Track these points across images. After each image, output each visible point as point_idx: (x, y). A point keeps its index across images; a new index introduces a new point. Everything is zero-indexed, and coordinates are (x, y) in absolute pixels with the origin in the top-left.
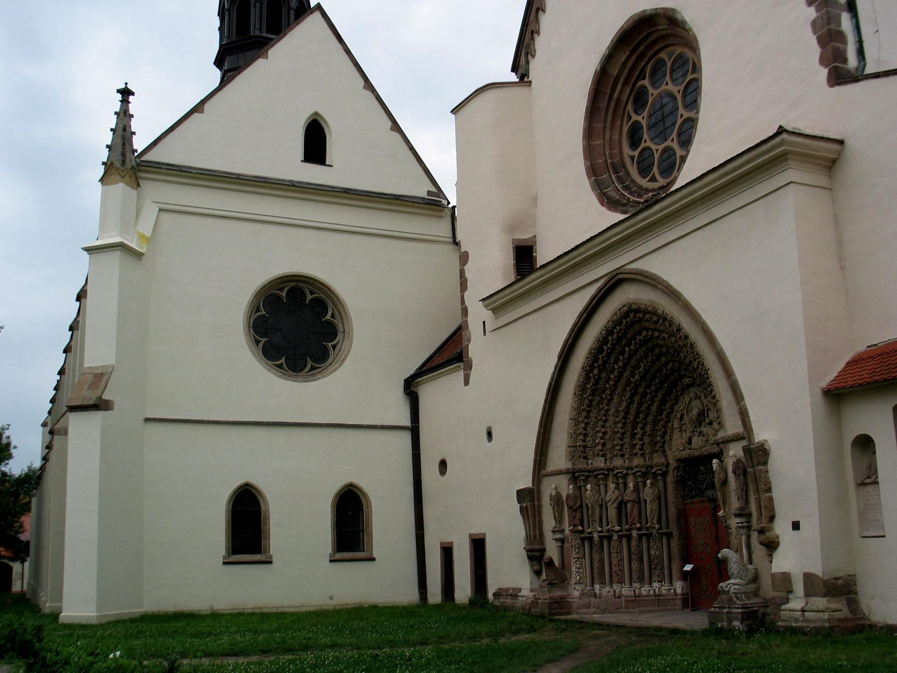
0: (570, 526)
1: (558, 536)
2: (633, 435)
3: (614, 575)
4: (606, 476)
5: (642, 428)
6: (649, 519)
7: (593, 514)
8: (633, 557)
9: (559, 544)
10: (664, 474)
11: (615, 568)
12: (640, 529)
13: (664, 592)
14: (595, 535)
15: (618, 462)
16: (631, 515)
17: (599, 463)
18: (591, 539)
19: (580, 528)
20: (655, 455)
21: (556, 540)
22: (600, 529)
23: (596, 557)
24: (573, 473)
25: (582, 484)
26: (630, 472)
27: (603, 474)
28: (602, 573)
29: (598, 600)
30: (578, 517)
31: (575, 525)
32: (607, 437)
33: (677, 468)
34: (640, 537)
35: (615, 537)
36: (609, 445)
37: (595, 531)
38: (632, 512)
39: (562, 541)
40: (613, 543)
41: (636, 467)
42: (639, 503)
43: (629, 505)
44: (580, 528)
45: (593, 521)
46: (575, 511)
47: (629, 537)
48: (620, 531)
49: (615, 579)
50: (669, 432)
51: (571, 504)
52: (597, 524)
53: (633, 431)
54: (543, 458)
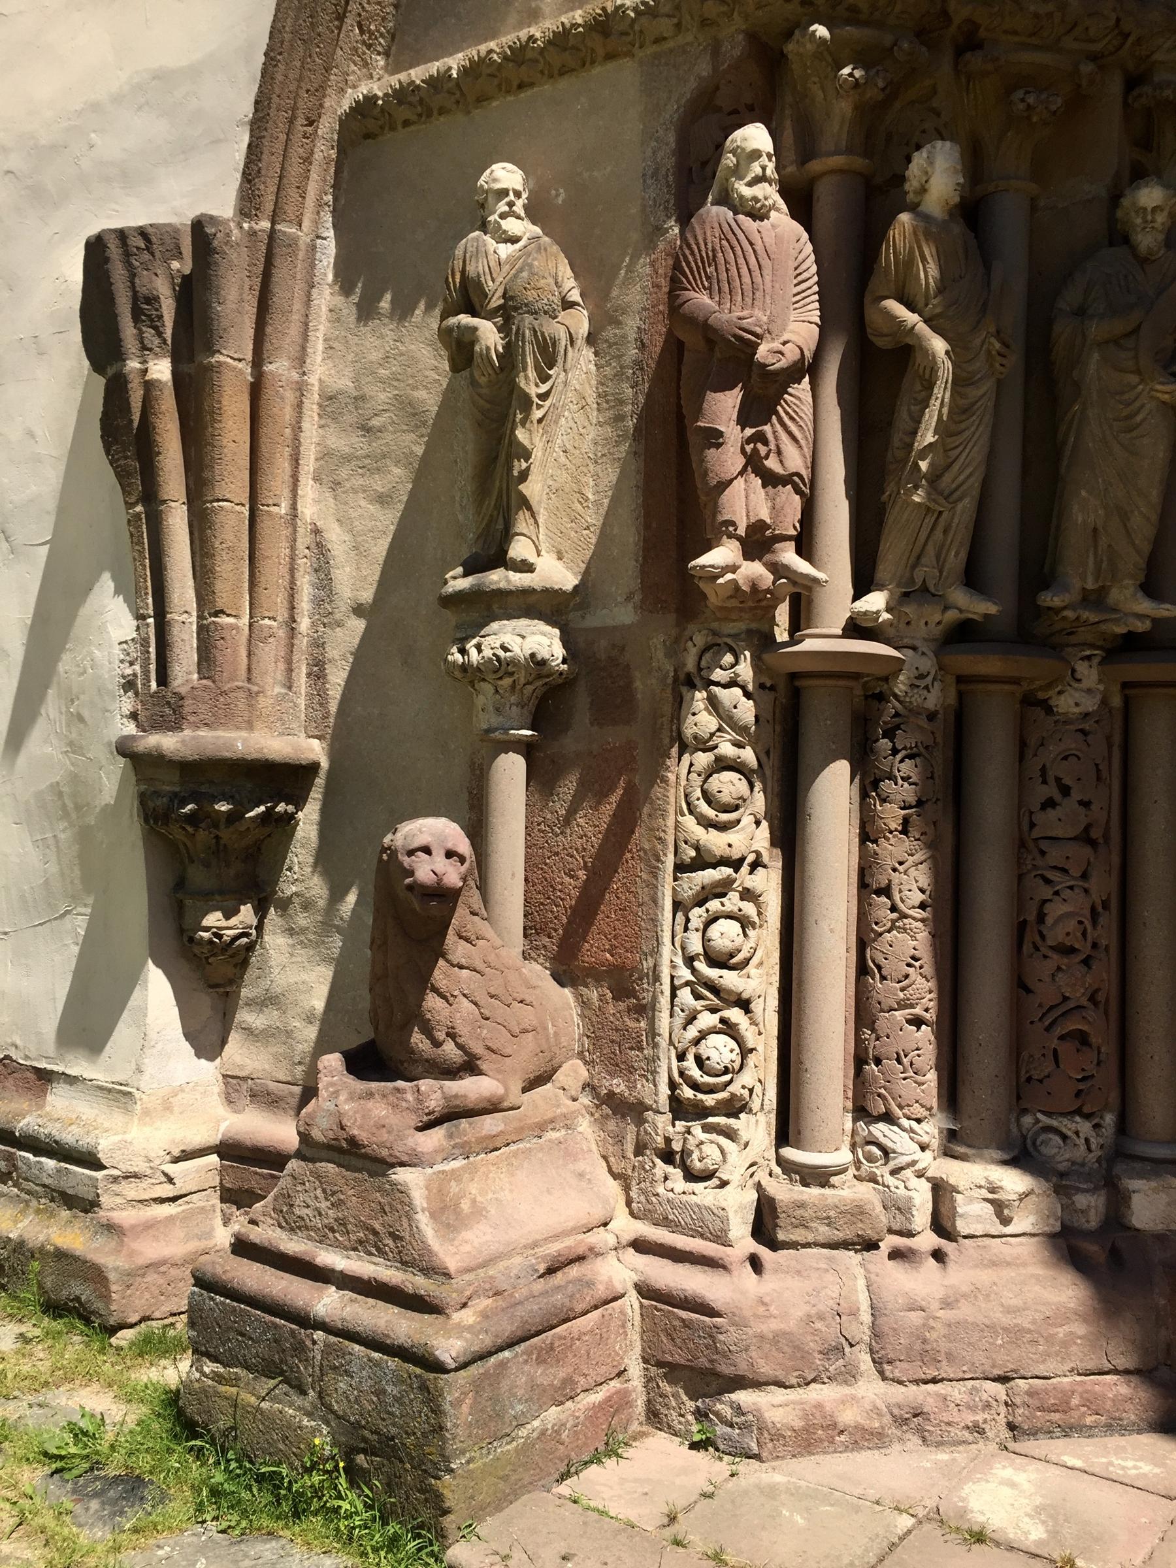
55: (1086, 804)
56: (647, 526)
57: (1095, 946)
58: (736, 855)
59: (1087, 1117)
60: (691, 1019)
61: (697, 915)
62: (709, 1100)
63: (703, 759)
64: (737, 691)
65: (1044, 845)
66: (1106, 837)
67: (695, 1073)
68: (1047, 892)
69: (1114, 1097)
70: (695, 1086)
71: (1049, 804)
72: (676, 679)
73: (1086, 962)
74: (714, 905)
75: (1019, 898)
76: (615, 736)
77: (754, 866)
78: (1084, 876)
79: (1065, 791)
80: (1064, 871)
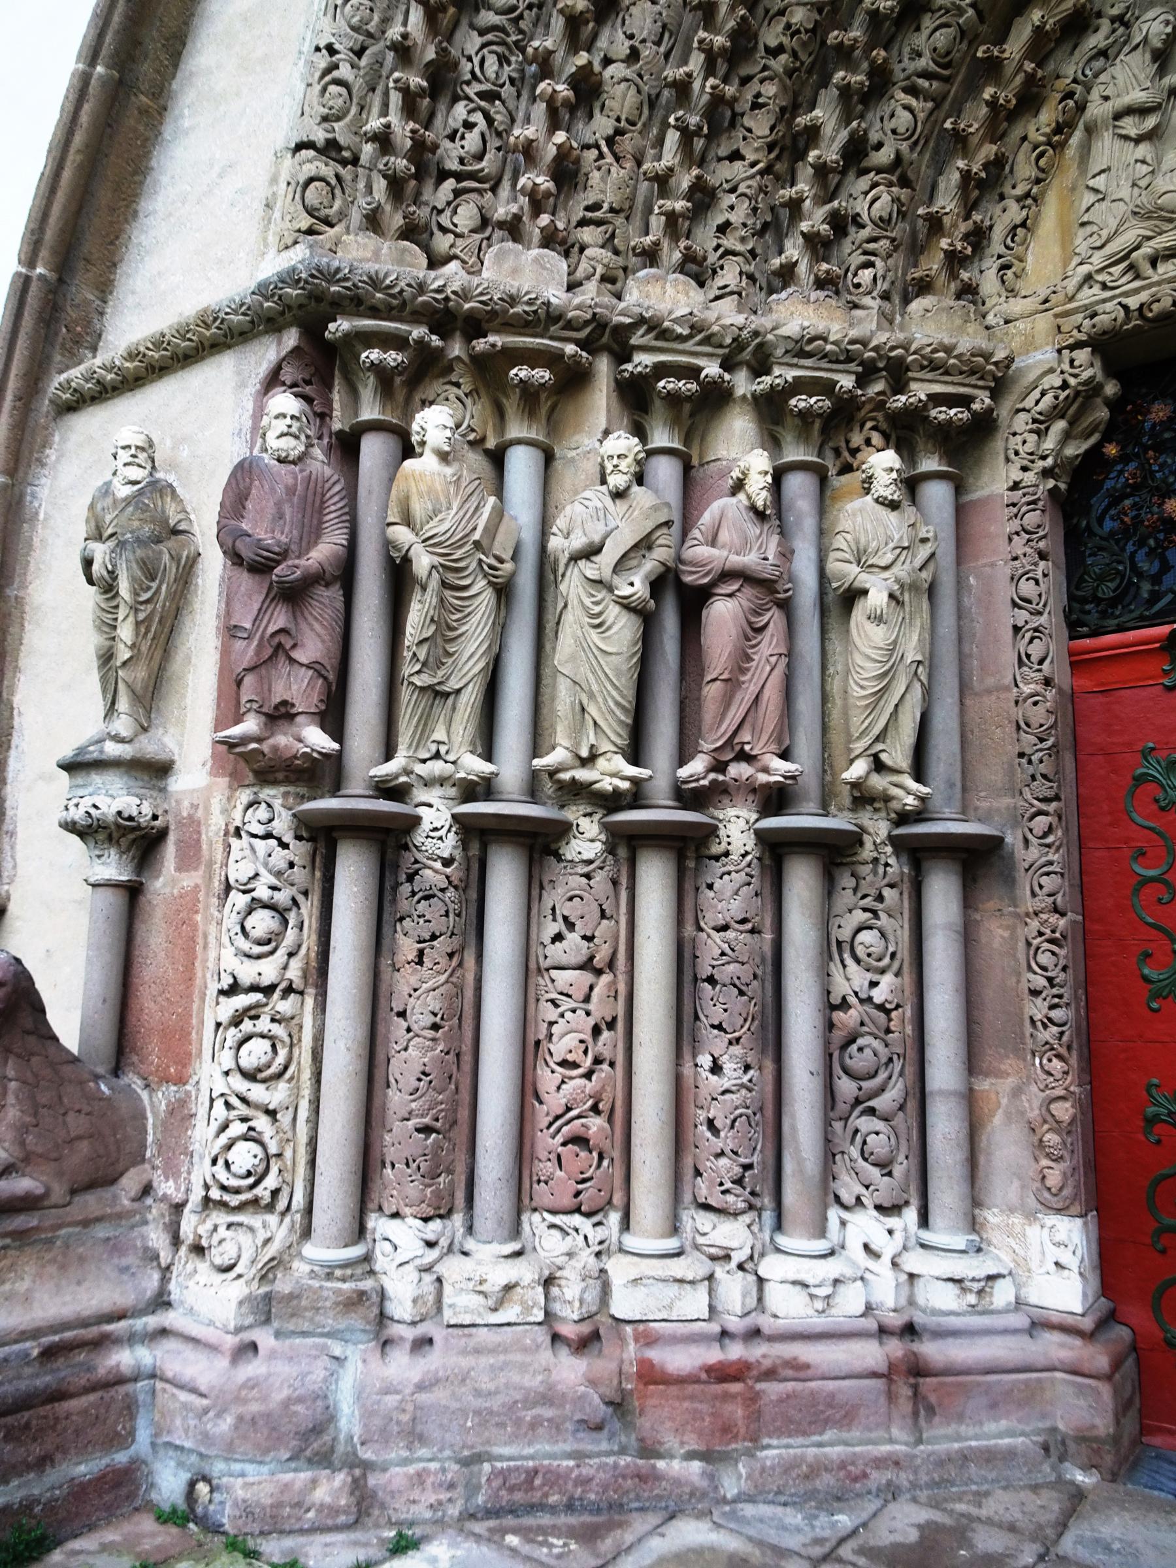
0: (229, 712)
1: (114, 798)
2: (791, 146)
3: (547, 1142)
4: (572, 380)
5: (855, 103)
6: (861, 726)
7: (444, 633)
8: (717, 1006)
9: (113, 867)
10: (966, 442)
11: (558, 1090)
12: (776, 799)
13: (941, 1299)
14: (435, 814)
15: (663, 295)
16: (733, 684)
17: (525, 273)
18: (389, 839)
19: (317, 739)
20: (916, 306)
21: (89, 831)
22: (474, 765)
23: (420, 992)
24: (313, 330)
25: (370, 412)
26: (743, 384)
27: (551, 359)
28: (454, 1125)
29: (402, 1367)
30: (313, 646)
31: (280, 715)
32: (602, 125)
33: (1074, 404)
34: (775, 851)
35: (587, 841)
36: (604, 184)
37: (436, 768)
38: (742, 661)
39: (141, 842)
40: (564, 889)
41: (801, 349)
42: (786, 606)
43: (724, 614)
44: (317, 739)
45: (437, 694)
46: (293, 595)
47: (690, 849)
48: (636, 796)
49: (558, 1183)
50: (1024, 169)
51: (262, 529)
52: (456, 729)
53: (788, 113)
54: (82, 291)
55: (588, 939)
56: (218, 705)
57: (598, 1061)
58: (266, 981)
59: (588, 1215)
60: (225, 1127)
61: (233, 1035)
62: (234, 1200)
63: (239, 900)
64: (273, 842)
65: (554, 973)
66: (611, 964)
67: (223, 1176)
68: (551, 1014)
69: (618, 1198)
70: (224, 1188)
71: (558, 938)
72: (226, 834)
73: (588, 1075)
74: (247, 1026)
75: (525, 1020)
76: (189, 880)
77: (289, 990)
78: (587, 999)
79: (571, 926)
80: (569, 996)
